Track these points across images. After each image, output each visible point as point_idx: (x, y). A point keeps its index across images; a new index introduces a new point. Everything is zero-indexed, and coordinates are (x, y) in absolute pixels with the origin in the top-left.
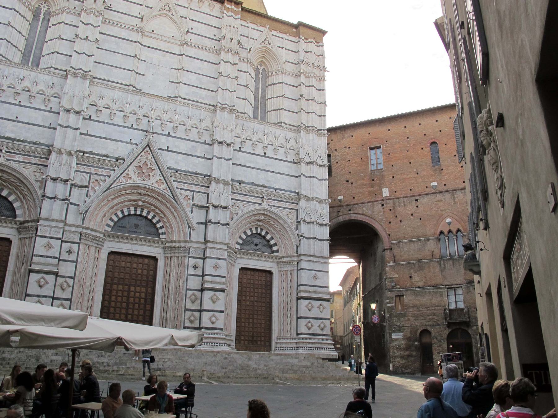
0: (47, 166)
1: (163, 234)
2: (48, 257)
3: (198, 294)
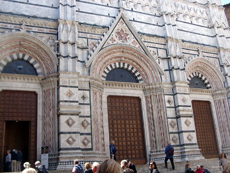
0: (57, 34)
1: (140, 80)
2: (71, 102)
3: (175, 120)
